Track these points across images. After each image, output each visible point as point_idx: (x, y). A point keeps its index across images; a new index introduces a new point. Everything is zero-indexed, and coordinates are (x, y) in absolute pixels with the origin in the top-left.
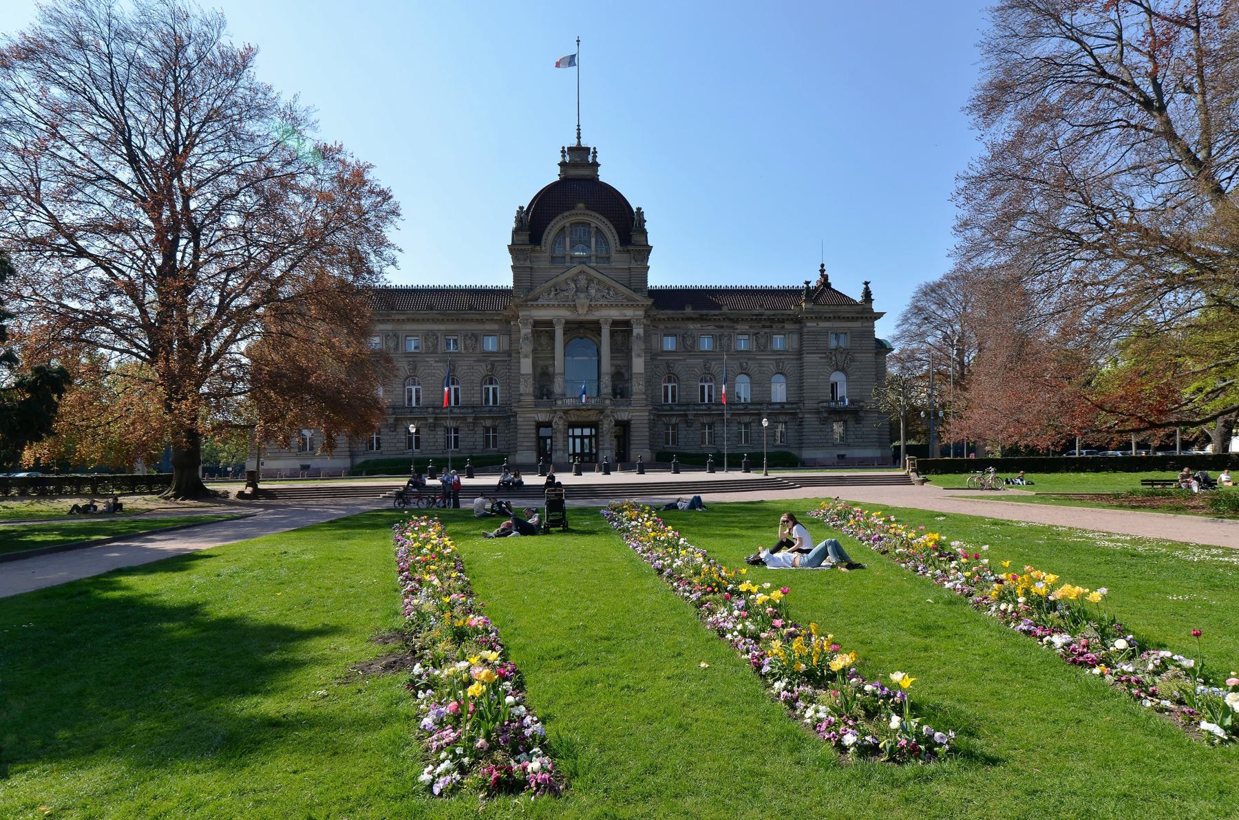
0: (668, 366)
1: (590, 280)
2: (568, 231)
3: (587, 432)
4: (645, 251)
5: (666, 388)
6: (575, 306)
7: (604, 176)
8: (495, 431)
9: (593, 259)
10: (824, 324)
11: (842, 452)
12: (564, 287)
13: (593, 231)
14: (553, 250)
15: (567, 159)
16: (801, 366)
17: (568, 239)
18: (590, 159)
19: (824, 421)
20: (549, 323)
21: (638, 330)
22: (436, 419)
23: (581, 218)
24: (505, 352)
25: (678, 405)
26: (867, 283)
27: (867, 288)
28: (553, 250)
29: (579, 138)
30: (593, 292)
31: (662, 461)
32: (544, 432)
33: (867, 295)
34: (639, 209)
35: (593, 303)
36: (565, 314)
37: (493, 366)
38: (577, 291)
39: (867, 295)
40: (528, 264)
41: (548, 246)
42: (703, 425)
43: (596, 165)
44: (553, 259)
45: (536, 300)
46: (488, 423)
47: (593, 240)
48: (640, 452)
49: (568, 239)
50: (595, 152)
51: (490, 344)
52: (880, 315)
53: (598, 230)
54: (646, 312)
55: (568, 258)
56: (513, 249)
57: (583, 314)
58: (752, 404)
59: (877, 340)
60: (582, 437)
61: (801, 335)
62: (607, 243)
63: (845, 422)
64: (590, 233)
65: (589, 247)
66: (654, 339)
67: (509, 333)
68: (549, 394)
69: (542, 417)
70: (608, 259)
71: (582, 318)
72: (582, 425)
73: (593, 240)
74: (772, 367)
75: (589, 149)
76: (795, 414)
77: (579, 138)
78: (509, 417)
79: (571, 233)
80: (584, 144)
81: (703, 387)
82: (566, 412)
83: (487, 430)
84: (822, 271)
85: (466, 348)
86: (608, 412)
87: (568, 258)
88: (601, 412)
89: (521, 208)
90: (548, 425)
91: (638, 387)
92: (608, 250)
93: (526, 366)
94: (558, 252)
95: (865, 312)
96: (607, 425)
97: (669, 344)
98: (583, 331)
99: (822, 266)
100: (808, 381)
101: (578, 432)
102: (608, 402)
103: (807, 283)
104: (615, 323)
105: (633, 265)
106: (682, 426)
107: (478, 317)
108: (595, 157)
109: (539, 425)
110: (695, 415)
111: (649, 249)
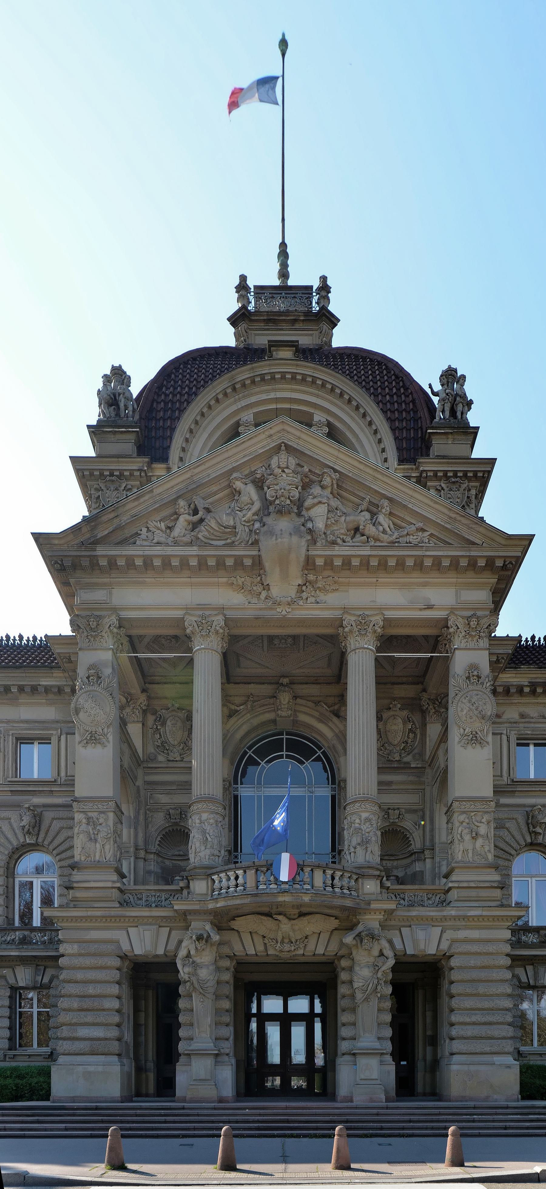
45: (130, 540)
86: (371, 921)
88: (347, 919)
96: (367, 977)
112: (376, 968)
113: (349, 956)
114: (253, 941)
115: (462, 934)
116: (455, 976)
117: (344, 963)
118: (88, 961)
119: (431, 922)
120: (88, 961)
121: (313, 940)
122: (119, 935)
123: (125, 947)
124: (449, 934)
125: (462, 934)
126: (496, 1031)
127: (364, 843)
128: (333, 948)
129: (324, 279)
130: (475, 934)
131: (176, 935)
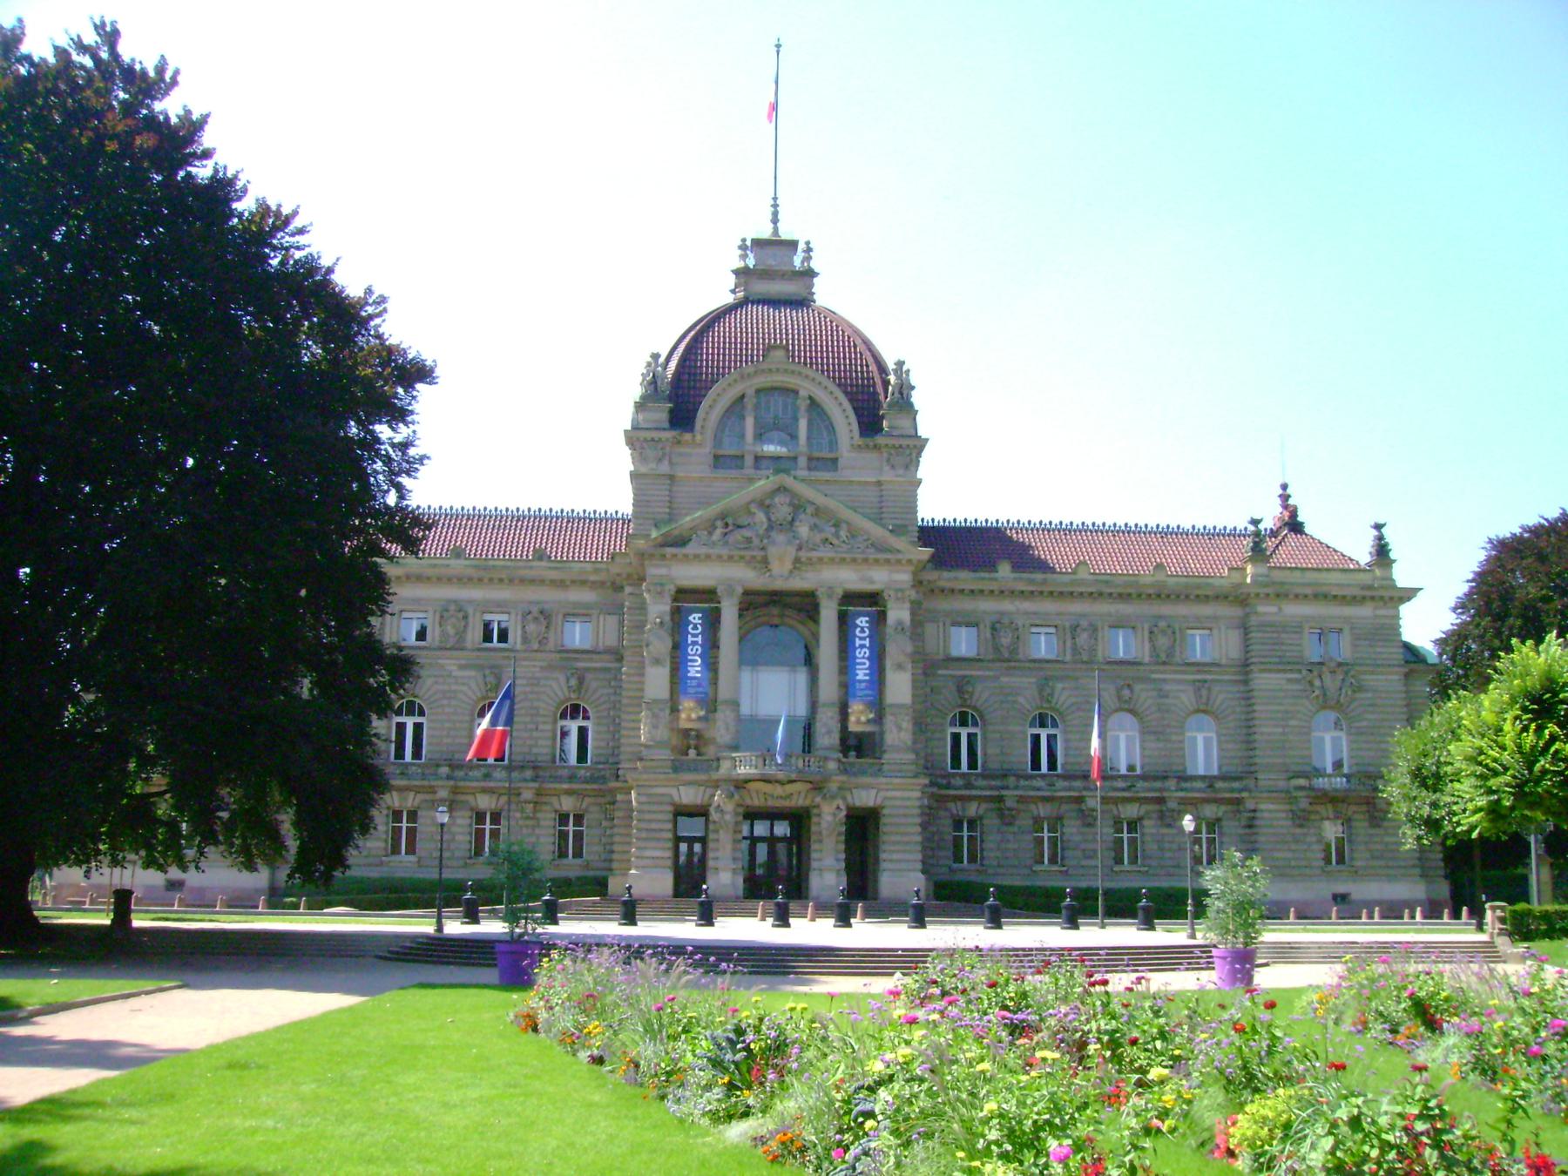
0: (960, 690)
1: (798, 506)
2: (750, 402)
3: (782, 829)
4: (913, 447)
5: (956, 738)
6: (765, 562)
7: (824, 294)
8: (579, 819)
9: (802, 462)
10: (1294, 610)
11: (1341, 888)
12: (744, 521)
13: (803, 405)
14: (717, 440)
15: (751, 262)
16: (1248, 698)
17: (750, 422)
18: (797, 261)
19: (1301, 819)
20: (707, 595)
21: (898, 614)
22: (455, 791)
23: (778, 379)
24: (609, 651)
25: (984, 776)
26: (1378, 527)
27: (1380, 538)
29: (775, 221)
30: (803, 530)
31: (953, 896)
33: (1382, 551)
34: (900, 364)
35: (803, 555)
36: (746, 576)
37: (581, 680)
38: (770, 528)
39: (1382, 551)
40: (664, 468)
41: (710, 433)
42: (1038, 822)
43: (810, 274)
44: (719, 461)
46: (567, 804)
47: (803, 424)
48: (901, 873)
49: (750, 422)
50: (809, 250)
51: (577, 635)
52: (1409, 594)
53: (813, 404)
54: (915, 574)
55: (749, 461)
56: (635, 438)
57: (781, 576)
58: (1144, 777)
59: (1408, 647)
60: (772, 840)
61: (1245, 629)
62: (831, 428)
63: (1348, 822)
64: (796, 409)
65: (794, 437)
66: (930, 629)
67: (617, 609)
69: (689, 796)
70: (835, 461)
71: (779, 585)
72: (772, 816)
73: (803, 424)
74: (1186, 699)
75: (793, 245)
76: (1238, 802)
77: (775, 221)
78: (612, 792)
79: (757, 407)
80: (785, 234)
81: (1036, 738)
82: (741, 784)
83: (563, 819)
84: (1285, 498)
85: (525, 640)
86: (833, 786)
87: (749, 461)
89: (656, 356)
90: (701, 812)
91: (898, 734)
92: (833, 444)
95: (1376, 588)
97: (963, 643)
98: (780, 613)
99: (1284, 487)
100: (1266, 730)
101: (761, 829)
102: (832, 765)
103: (1255, 522)
104: (850, 598)
105: (887, 476)
106: (991, 822)
107: (554, 575)
108: (808, 259)
109: (681, 812)
110: (1021, 799)
111: (919, 445)
112: (834, 815)
113: (818, 806)
114: (757, 798)
115: (890, 794)
116: (883, 820)
117: (815, 811)
118: (654, 808)
119: (867, 787)
120: (654, 808)
121: (797, 796)
122: (673, 792)
123: (676, 799)
124: (882, 794)
125: (890, 794)
126: (907, 856)
127: (829, 732)
128: (808, 803)
129: (808, 243)
130: (898, 794)
131: (709, 791)
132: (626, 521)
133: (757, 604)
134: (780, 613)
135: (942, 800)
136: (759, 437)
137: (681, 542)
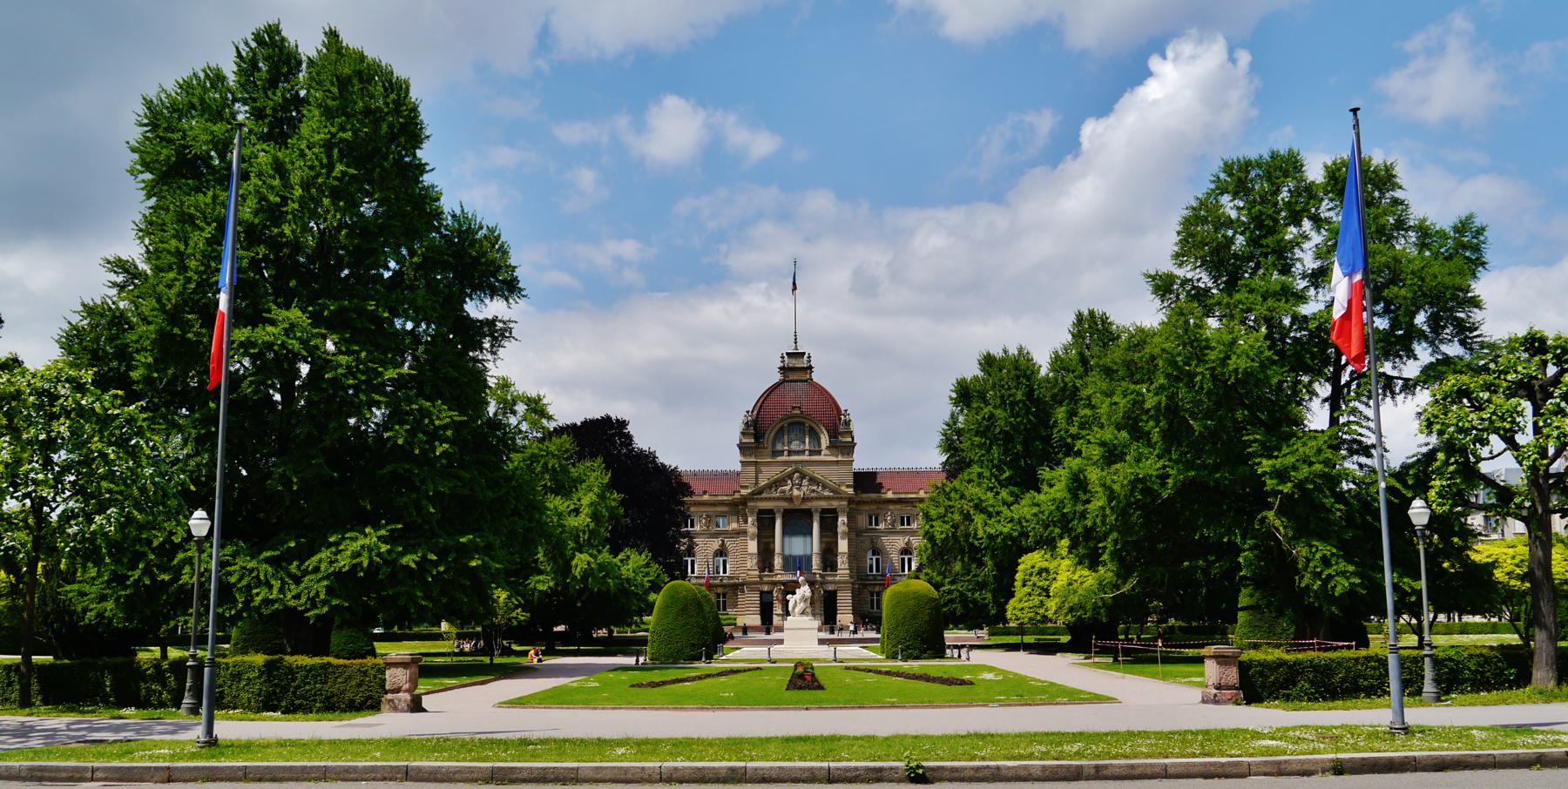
1: (803, 476)
7: (816, 377)
20: (771, 512)
28: (774, 445)
32: (766, 600)
36: (785, 505)
43: (810, 368)
46: (720, 590)
56: (743, 448)
57: (797, 505)
68: (771, 568)
69: (766, 588)
91: (842, 562)
92: (819, 444)
93: (753, 546)
94: (779, 447)
104: (824, 511)
109: (762, 593)
132: (738, 474)
133: (788, 515)
134: (797, 521)
135: (865, 586)
136: (790, 443)
137: (760, 493)
